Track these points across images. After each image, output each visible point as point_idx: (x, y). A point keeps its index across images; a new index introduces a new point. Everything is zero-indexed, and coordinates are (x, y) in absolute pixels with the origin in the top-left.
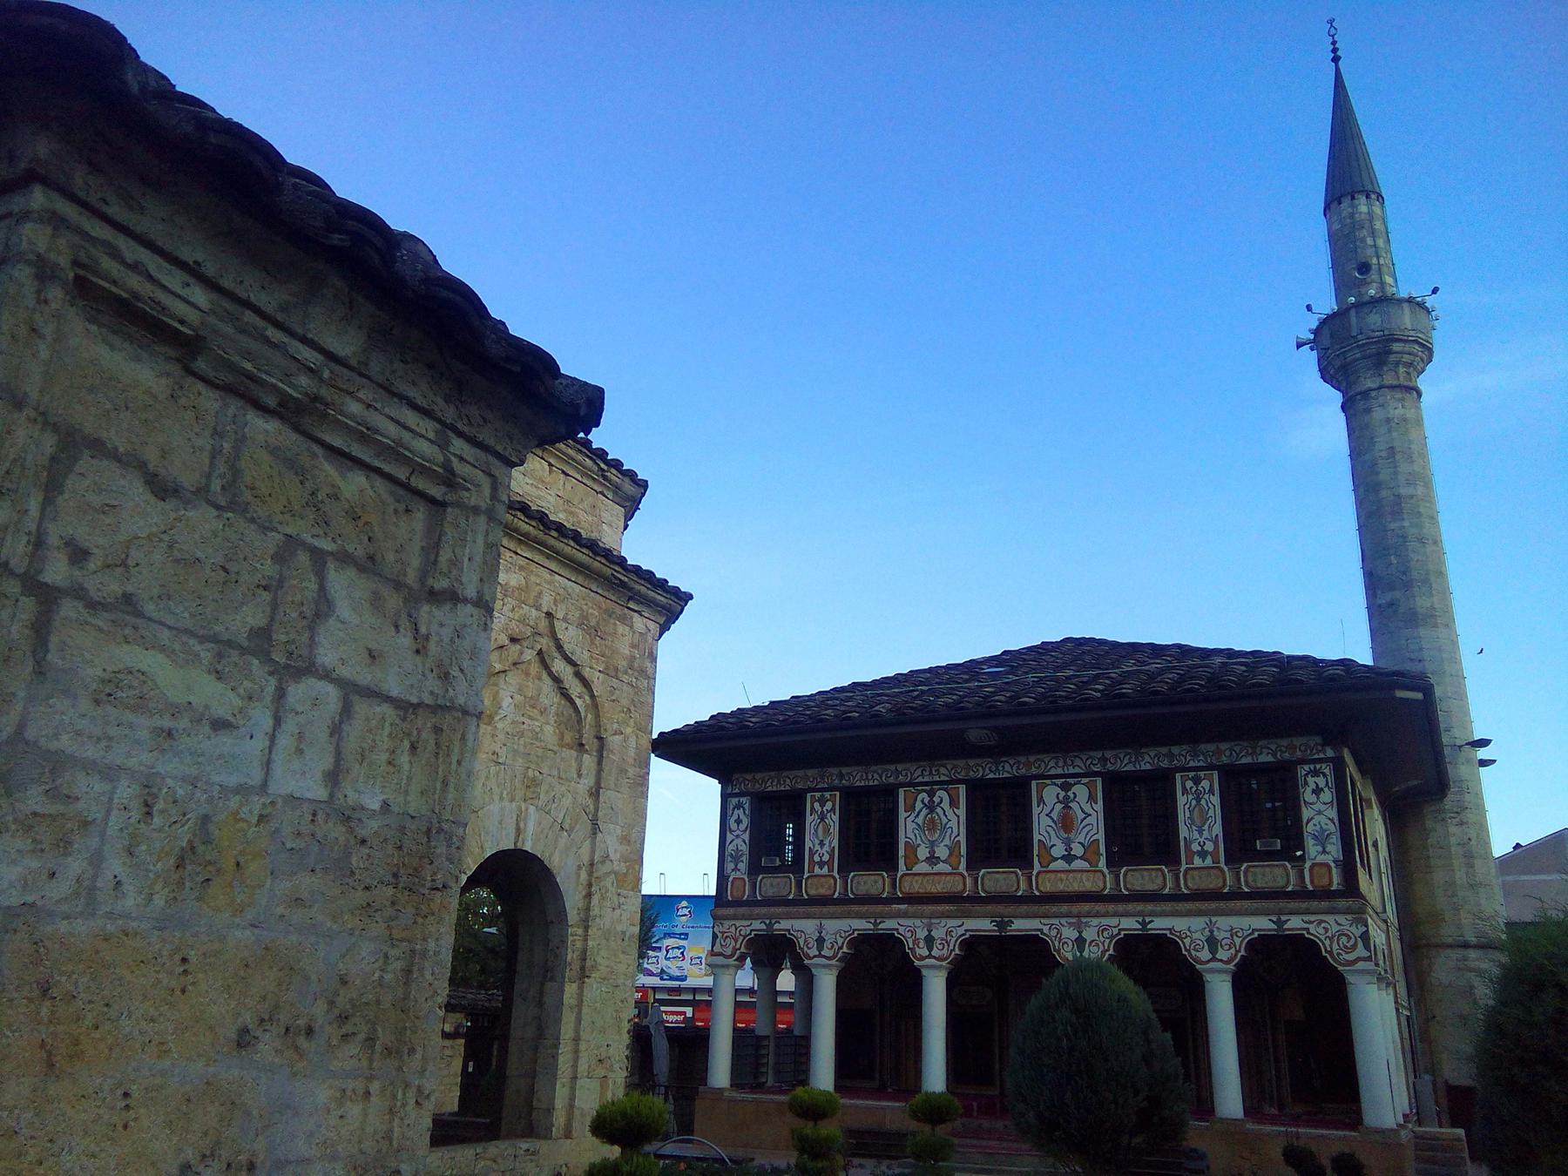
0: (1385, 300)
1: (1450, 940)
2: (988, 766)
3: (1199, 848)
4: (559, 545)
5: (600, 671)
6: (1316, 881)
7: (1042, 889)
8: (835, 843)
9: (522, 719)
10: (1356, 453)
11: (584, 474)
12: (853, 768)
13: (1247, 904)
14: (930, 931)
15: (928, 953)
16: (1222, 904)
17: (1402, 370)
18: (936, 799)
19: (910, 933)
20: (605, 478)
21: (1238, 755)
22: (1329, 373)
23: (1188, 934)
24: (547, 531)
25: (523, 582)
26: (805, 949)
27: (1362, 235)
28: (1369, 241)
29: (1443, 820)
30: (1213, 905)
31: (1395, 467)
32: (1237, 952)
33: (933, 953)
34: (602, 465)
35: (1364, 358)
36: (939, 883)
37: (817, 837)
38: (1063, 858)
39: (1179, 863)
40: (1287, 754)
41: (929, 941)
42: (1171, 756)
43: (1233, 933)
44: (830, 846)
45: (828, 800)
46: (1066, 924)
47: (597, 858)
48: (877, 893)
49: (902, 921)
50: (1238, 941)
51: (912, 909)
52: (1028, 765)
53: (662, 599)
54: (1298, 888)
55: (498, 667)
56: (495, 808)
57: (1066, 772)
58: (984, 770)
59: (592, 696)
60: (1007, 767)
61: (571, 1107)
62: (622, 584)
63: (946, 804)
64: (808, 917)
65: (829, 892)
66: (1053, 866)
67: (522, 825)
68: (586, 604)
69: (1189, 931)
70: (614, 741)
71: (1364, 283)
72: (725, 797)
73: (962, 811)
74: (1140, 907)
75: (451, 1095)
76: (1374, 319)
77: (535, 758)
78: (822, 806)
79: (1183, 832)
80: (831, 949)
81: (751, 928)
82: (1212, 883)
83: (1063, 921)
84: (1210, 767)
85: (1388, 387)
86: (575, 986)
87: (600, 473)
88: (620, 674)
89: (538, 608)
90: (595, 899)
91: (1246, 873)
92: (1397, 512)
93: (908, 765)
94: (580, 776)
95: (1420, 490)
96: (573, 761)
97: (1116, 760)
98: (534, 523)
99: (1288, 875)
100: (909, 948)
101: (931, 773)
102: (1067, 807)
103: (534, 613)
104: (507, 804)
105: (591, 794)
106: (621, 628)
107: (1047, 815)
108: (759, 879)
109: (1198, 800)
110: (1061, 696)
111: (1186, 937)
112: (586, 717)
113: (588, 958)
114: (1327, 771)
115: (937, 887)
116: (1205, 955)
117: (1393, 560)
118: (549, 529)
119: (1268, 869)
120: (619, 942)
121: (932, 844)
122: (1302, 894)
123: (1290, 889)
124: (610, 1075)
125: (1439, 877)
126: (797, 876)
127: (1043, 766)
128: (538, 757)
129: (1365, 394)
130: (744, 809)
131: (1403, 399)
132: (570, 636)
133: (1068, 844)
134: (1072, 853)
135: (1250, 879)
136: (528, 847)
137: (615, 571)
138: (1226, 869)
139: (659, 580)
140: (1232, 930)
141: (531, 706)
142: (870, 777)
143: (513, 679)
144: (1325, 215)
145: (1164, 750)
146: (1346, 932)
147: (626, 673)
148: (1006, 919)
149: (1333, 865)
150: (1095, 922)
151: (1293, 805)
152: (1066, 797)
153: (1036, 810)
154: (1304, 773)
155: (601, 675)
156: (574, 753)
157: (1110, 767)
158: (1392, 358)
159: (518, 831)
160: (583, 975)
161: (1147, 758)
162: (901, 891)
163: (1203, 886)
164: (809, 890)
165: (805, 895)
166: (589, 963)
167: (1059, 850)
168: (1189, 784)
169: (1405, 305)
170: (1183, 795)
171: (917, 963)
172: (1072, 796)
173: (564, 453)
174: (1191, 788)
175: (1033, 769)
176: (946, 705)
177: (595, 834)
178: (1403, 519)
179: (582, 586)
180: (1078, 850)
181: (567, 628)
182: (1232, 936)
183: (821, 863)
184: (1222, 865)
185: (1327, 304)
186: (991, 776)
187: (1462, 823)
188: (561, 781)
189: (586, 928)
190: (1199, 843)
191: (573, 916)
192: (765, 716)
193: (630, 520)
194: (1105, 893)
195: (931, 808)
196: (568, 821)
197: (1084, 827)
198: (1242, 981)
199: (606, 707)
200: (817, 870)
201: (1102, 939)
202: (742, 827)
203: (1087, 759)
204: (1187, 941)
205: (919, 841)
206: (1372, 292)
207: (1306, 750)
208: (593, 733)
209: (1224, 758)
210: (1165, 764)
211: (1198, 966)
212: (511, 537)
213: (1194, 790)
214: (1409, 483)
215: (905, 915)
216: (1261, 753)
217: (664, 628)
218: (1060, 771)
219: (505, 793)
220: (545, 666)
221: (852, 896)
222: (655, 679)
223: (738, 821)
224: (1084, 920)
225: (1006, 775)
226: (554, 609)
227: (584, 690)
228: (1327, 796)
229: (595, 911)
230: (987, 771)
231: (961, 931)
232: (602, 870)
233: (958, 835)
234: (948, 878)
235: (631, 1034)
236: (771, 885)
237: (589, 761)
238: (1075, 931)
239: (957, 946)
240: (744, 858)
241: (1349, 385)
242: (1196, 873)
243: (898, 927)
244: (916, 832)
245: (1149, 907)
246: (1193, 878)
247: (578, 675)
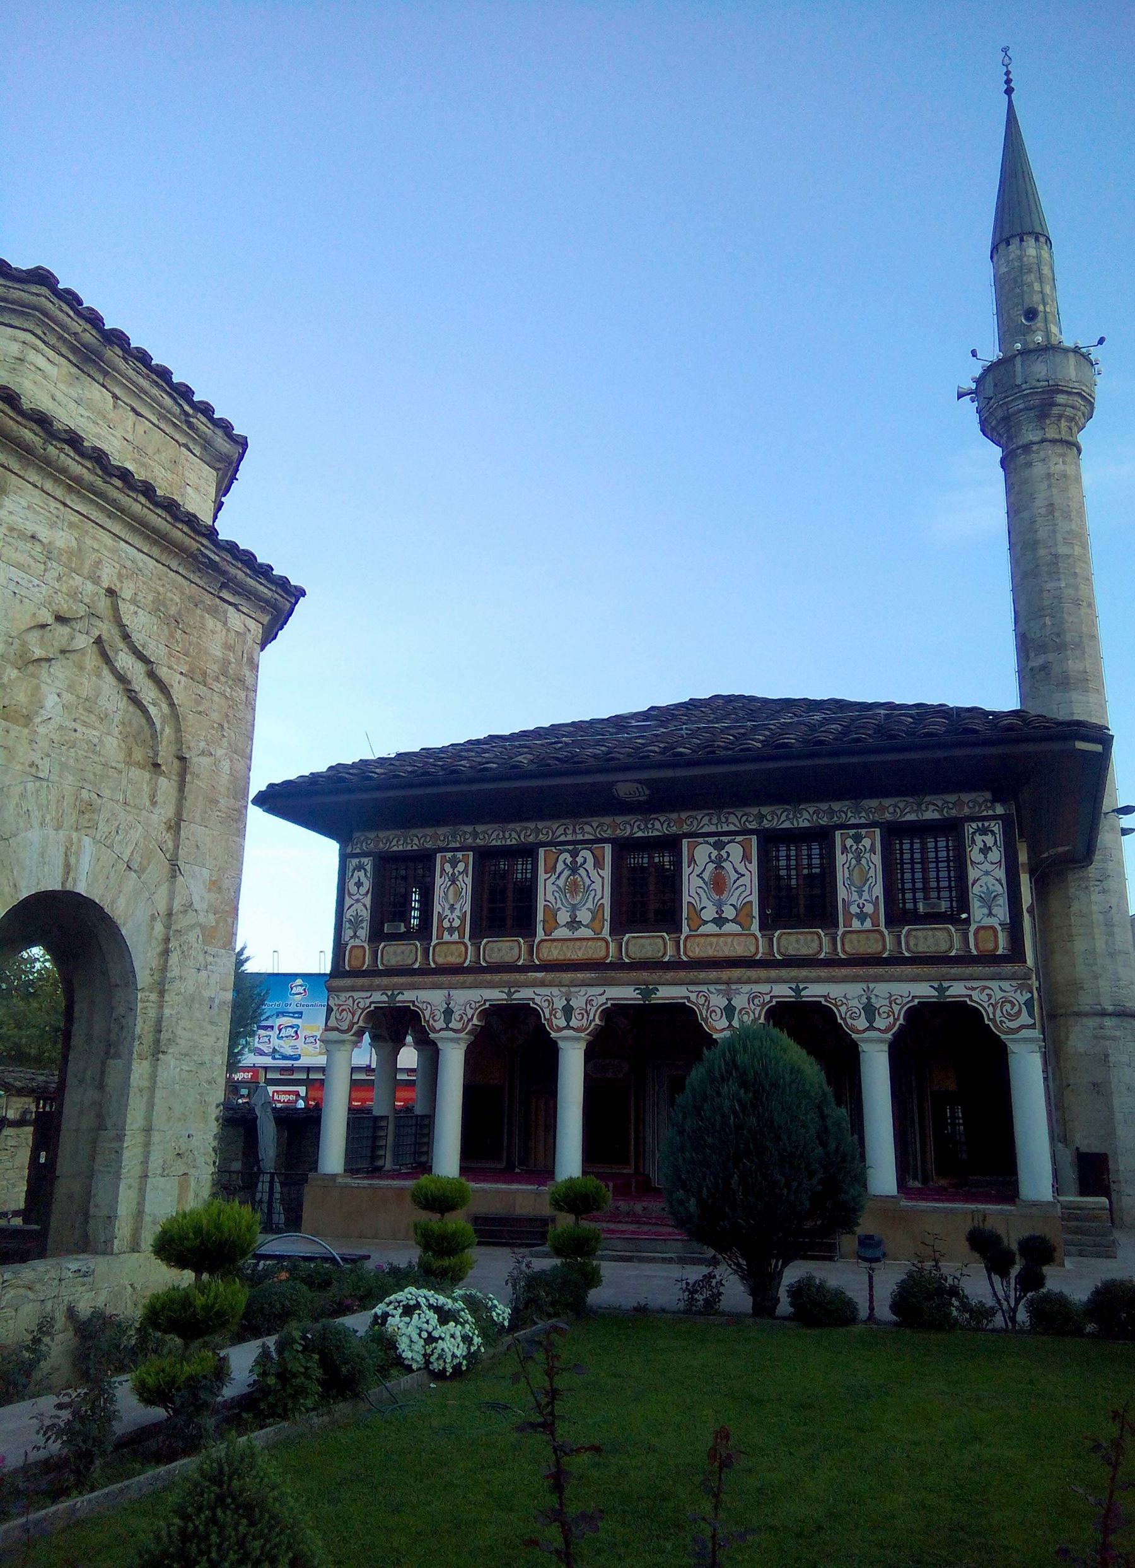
0: (1051, 349)
1: (1088, 1008)
2: (637, 824)
3: (858, 911)
4: (125, 500)
5: (181, 673)
6: (980, 945)
7: (690, 954)
8: (467, 908)
9: (74, 725)
10: (1014, 511)
11: (161, 417)
12: (489, 826)
13: (909, 970)
14: (568, 1000)
15: (565, 1024)
16: (880, 970)
17: (1063, 423)
18: (579, 860)
19: (547, 1003)
20: (191, 426)
21: (902, 812)
22: (987, 428)
23: (845, 1001)
24: (108, 479)
25: (74, 544)
26: (431, 1022)
27: (1029, 280)
28: (1037, 287)
29: (1087, 887)
30: (872, 971)
31: (1055, 525)
32: (896, 1020)
33: (571, 1024)
34: (187, 408)
35: (1027, 409)
36: (580, 949)
38: (714, 921)
39: (837, 926)
40: (954, 811)
41: (568, 1011)
42: (832, 812)
43: (891, 1000)
44: (461, 910)
45: (460, 861)
46: (714, 991)
47: (176, 907)
48: (512, 960)
49: (538, 990)
50: (896, 1008)
51: (550, 976)
52: (680, 822)
53: (266, 591)
54: (961, 953)
55: (38, 653)
56: (34, 835)
57: (720, 830)
58: (632, 827)
59: (172, 705)
60: (657, 825)
61: (140, 1213)
62: (213, 565)
63: (590, 865)
65: (459, 960)
66: (703, 929)
67: (73, 860)
68: (163, 586)
69: (845, 997)
70: (200, 764)
71: (1030, 330)
72: (344, 858)
73: (607, 873)
74: (794, 972)
75: (17, 1190)
76: (1040, 369)
77: (91, 777)
78: (454, 867)
79: (842, 893)
80: (460, 1021)
81: (371, 999)
82: (871, 947)
83: (712, 988)
84: (873, 825)
85: (1050, 441)
86: (146, 1064)
87: (183, 417)
88: (209, 681)
89: (96, 581)
90: (174, 958)
91: (907, 936)
92: (1054, 572)
93: (548, 823)
94: (154, 803)
95: (1077, 550)
96: (145, 786)
97: (773, 817)
98: (89, 465)
99: (951, 941)
100: (545, 1019)
101: (574, 831)
102: (719, 867)
103: (90, 587)
104: (52, 832)
105: (169, 828)
106: (210, 622)
107: (698, 876)
108: (381, 947)
109: (859, 860)
110: (719, 747)
111: (843, 1004)
112: (163, 730)
113: (164, 1029)
114: (997, 831)
115: (579, 953)
116: (862, 1023)
117: (1048, 621)
118: (111, 475)
119: (930, 933)
120: (206, 1009)
121: (574, 909)
122: (965, 959)
123: (953, 954)
124: (192, 1171)
125: (1080, 945)
126: (425, 943)
127: (695, 823)
128: (95, 774)
129: (1027, 448)
130: (365, 870)
131: (1063, 455)
132: (140, 623)
133: (719, 905)
134: (723, 916)
135: (912, 943)
136: (81, 888)
137: (203, 545)
138: (886, 932)
139: (261, 565)
140: (891, 996)
141: (85, 710)
142: (507, 835)
143: (60, 671)
144: (992, 258)
145: (824, 806)
146: (1011, 999)
147: (217, 679)
148: (651, 987)
149: (999, 928)
150: (746, 988)
151: (960, 863)
152: (720, 856)
153: (686, 871)
154: (971, 831)
155: (183, 678)
156: (147, 775)
157: (766, 824)
158: (1055, 411)
159: (68, 868)
160: (157, 1051)
161: (806, 815)
162: (538, 957)
163: (861, 950)
164: (436, 958)
165: (432, 963)
166: (164, 1036)
167: (709, 914)
168: (849, 842)
169: (1071, 355)
170: (842, 854)
171: (553, 1035)
172: (725, 856)
173: (133, 383)
174: (851, 846)
175: (685, 826)
176: (595, 756)
177: (174, 877)
178: (1059, 580)
179: (157, 561)
180: (729, 913)
181: (136, 613)
182: (891, 1004)
183: (451, 930)
184: (883, 928)
185: (991, 352)
186: (640, 834)
187: (1104, 891)
188: (128, 808)
189: (162, 993)
190: (858, 906)
191: (144, 977)
192: (392, 767)
193: (225, 495)
194: (758, 958)
195: (574, 870)
196: (137, 858)
197: (737, 889)
198: (899, 1051)
199: (190, 720)
200: (446, 937)
201: (753, 1007)
202: (363, 890)
203: (743, 816)
204: (843, 1009)
205: (559, 905)
206: (1039, 339)
207: (974, 807)
208: (173, 748)
209: (887, 815)
210: (824, 821)
211: (854, 1036)
212: (57, 480)
213: (855, 847)
214: (1066, 543)
215: (543, 984)
216: (927, 809)
217: (269, 636)
218: (713, 829)
219: (48, 817)
220: (107, 660)
221: (484, 964)
222: (255, 691)
223: (359, 884)
224: (734, 987)
225: (656, 833)
226: (118, 585)
227: (160, 696)
228: (995, 855)
229: (174, 972)
230: (635, 829)
231: (602, 999)
232: (181, 923)
233: (602, 898)
234: (590, 943)
235: (221, 1121)
236: (395, 954)
237: (166, 786)
238: (725, 999)
239: (597, 1017)
240: (364, 925)
241: (1010, 438)
242: (854, 936)
243: (533, 996)
244: (556, 894)
245: (804, 972)
246: (851, 941)
247: (152, 675)
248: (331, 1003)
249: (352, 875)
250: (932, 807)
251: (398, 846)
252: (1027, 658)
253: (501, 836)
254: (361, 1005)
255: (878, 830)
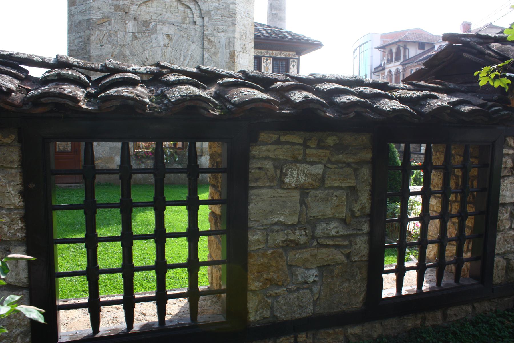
42: (261, 53)
84: (270, 57)
109: (267, 65)
145: (260, 51)
168: (265, 61)
210: (260, 55)
228: (296, 67)
250: (283, 55)
252: (271, 11)
255: (271, 59)
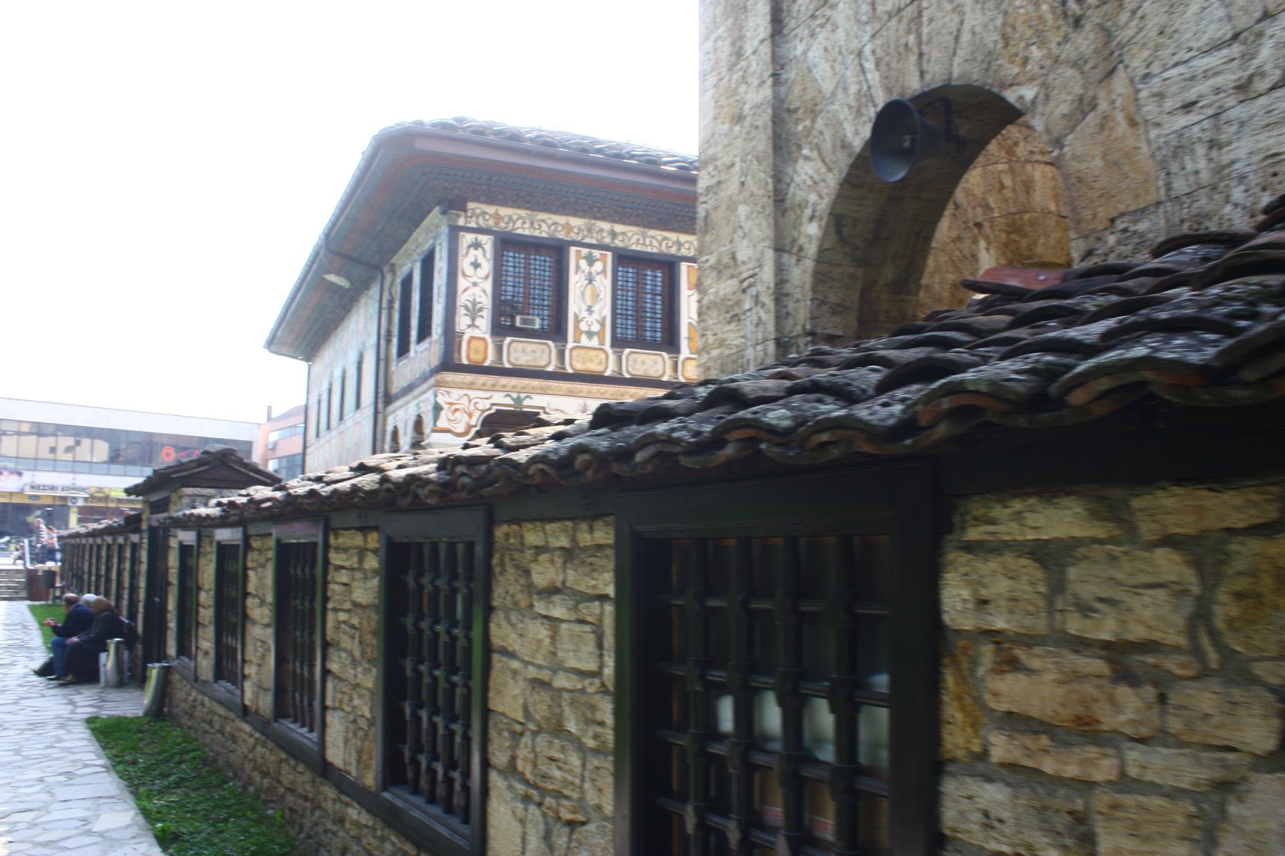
8: (607, 312)
37: (584, 301)
45: (597, 260)
64: (571, 394)
130: (483, 249)
142: (648, 243)
164: (574, 363)
183: (590, 334)
200: (585, 341)
223: (476, 265)
236: (523, 352)
248: (441, 400)
249: (467, 253)
251: (523, 230)
253: (641, 242)
254: (480, 406)
